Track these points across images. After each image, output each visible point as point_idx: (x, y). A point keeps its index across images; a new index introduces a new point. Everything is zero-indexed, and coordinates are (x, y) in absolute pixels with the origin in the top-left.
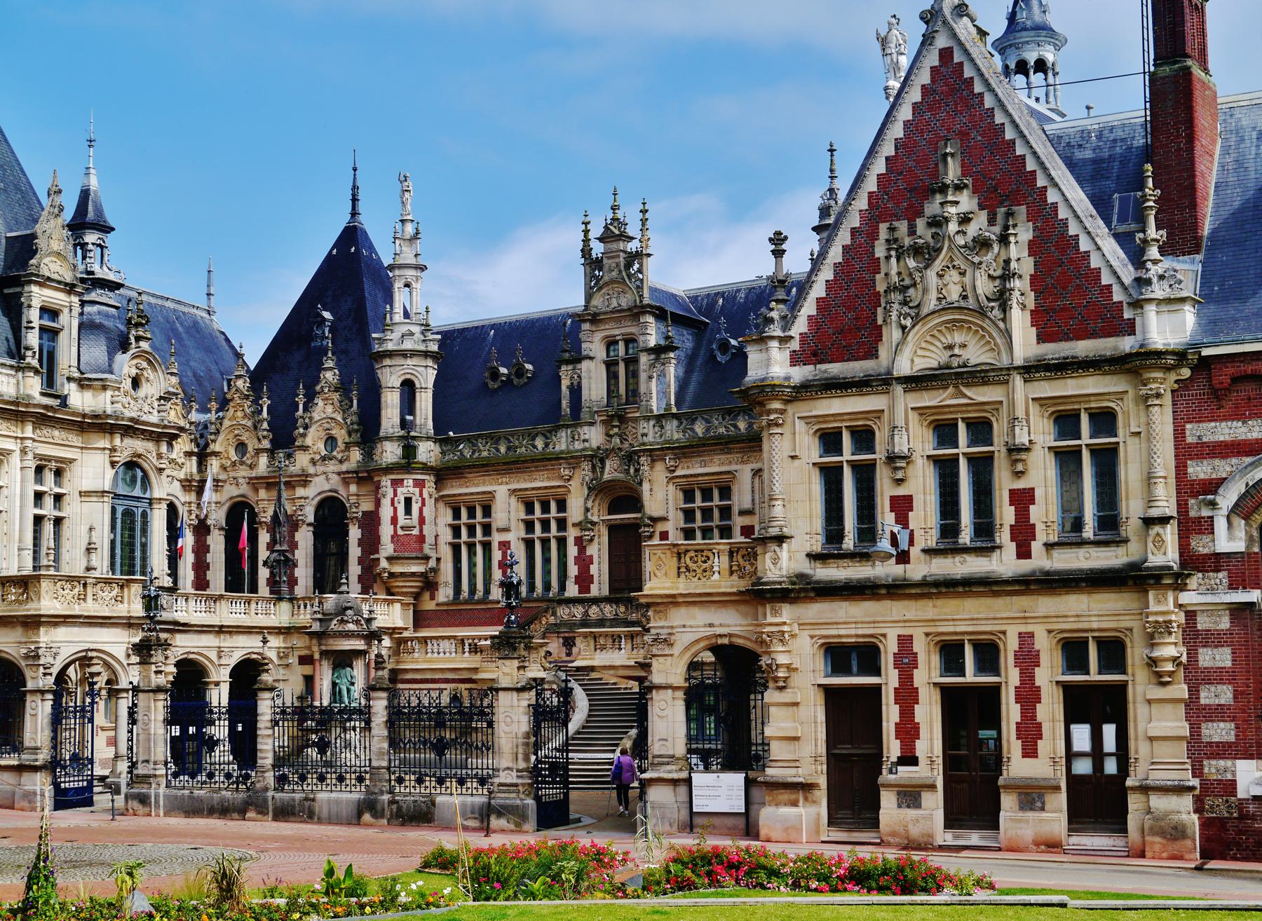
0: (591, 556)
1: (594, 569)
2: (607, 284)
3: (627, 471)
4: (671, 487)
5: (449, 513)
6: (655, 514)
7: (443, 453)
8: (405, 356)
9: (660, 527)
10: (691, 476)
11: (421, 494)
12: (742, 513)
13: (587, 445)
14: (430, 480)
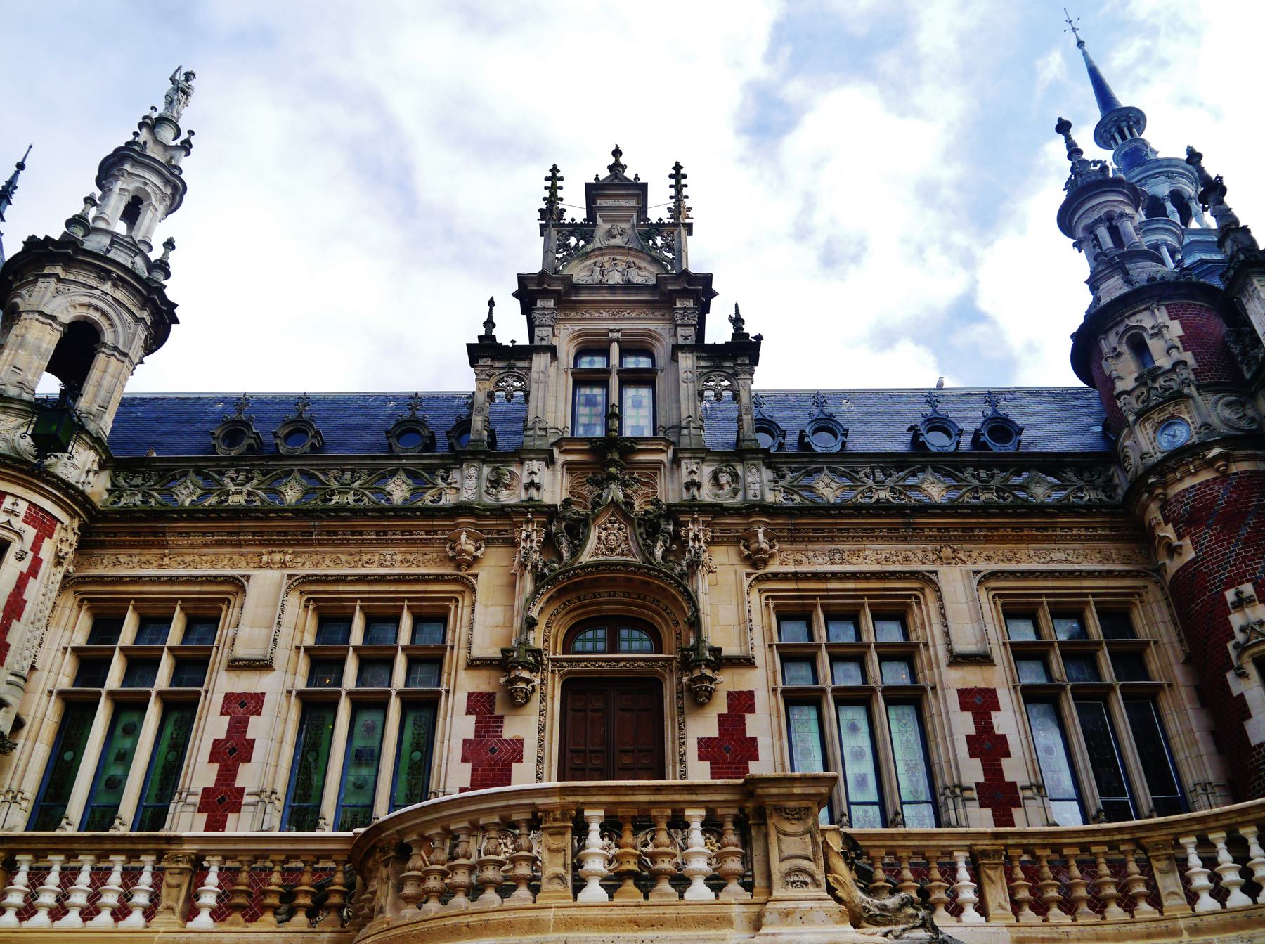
0: (517, 744)
3: (650, 549)
5: (84, 623)
7: (114, 490)
8: (104, 275)
9: (729, 681)
10: (816, 576)
11: (36, 547)
12: (958, 660)
13: (534, 493)
14: (67, 530)
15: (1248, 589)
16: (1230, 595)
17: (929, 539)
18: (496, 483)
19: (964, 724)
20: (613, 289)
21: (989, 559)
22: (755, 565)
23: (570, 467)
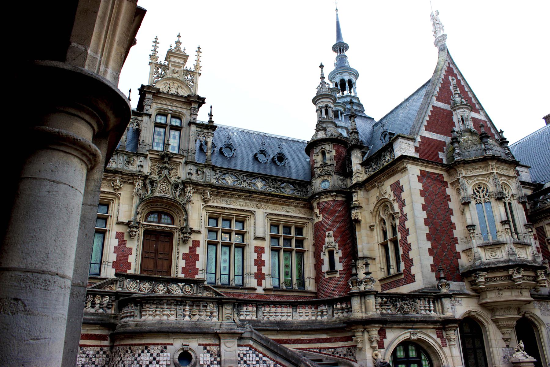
0: (131, 249)
1: (132, 259)
2: (169, 79)
4: (204, 213)
6: (195, 228)
9: (194, 237)
10: (222, 208)
12: (257, 238)
15: (331, 233)
16: (327, 233)
17: (256, 201)
18: (129, 163)
19: (255, 256)
20: (172, 95)
21: (270, 208)
22: (205, 202)
23: (152, 159)
